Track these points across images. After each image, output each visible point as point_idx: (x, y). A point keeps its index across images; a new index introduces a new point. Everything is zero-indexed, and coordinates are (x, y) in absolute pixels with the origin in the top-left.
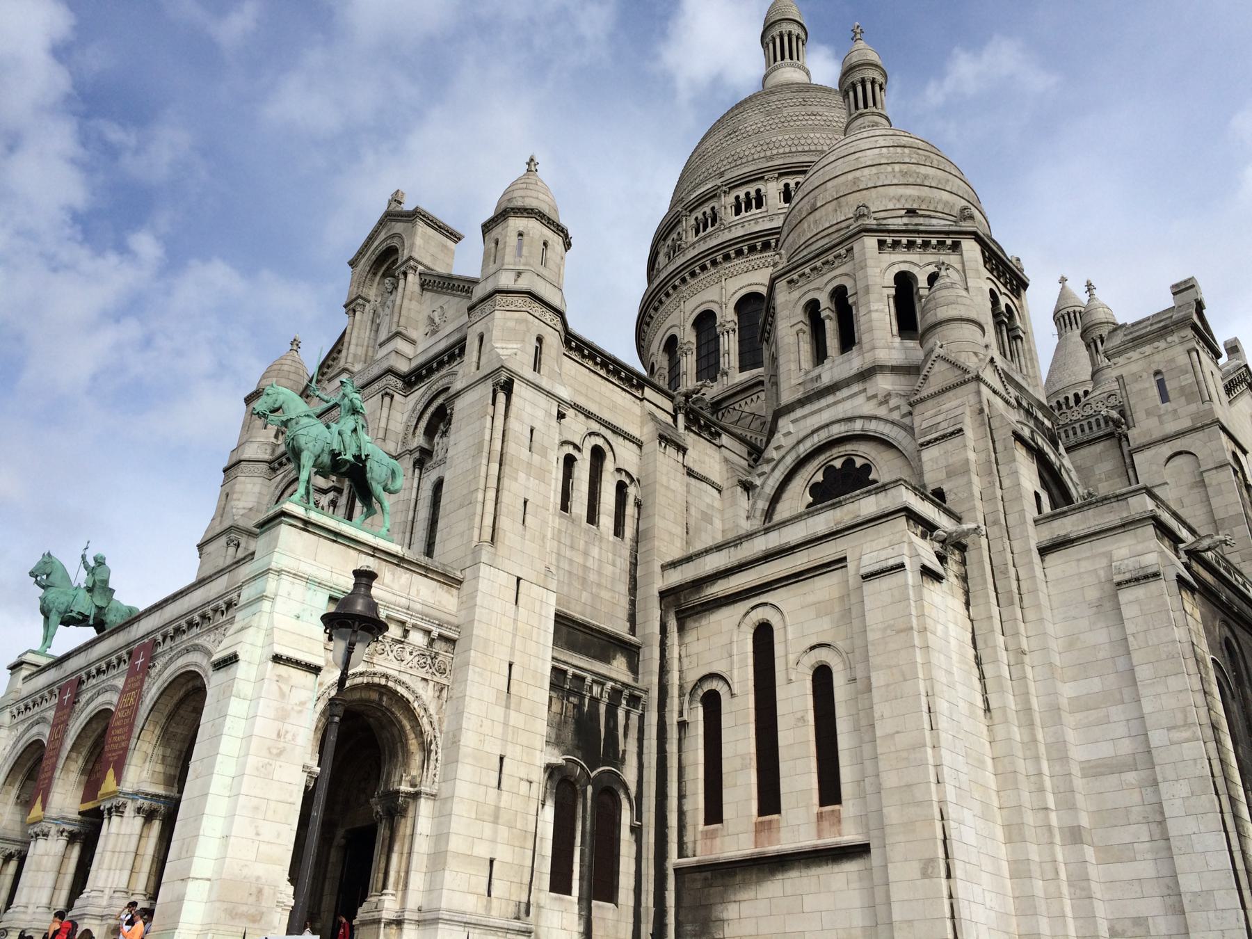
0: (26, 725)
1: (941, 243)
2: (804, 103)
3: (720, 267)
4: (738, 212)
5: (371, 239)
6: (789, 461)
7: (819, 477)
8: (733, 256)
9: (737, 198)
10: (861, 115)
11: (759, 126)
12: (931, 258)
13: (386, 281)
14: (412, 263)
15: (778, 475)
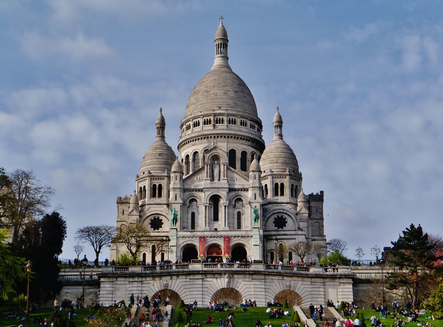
0: (185, 240)
1: (298, 179)
2: (242, 92)
3: (226, 139)
4: (230, 123)
5: (212, 150)
6: (272, 213)
7: (276, 217)
8: (230, 137)
9: (230, 119)
10: (279, 135)
11: (233, 96)
12: (296, 182)
13: (216, 162)
14: (226, 164)
15: (269, 215)
